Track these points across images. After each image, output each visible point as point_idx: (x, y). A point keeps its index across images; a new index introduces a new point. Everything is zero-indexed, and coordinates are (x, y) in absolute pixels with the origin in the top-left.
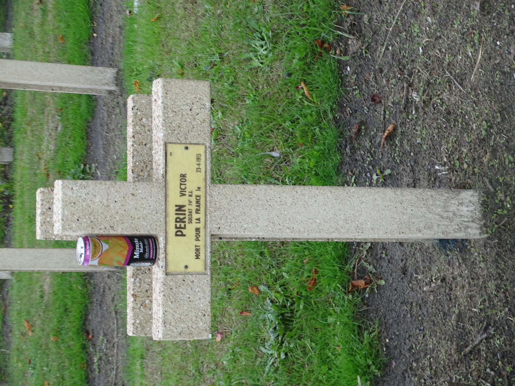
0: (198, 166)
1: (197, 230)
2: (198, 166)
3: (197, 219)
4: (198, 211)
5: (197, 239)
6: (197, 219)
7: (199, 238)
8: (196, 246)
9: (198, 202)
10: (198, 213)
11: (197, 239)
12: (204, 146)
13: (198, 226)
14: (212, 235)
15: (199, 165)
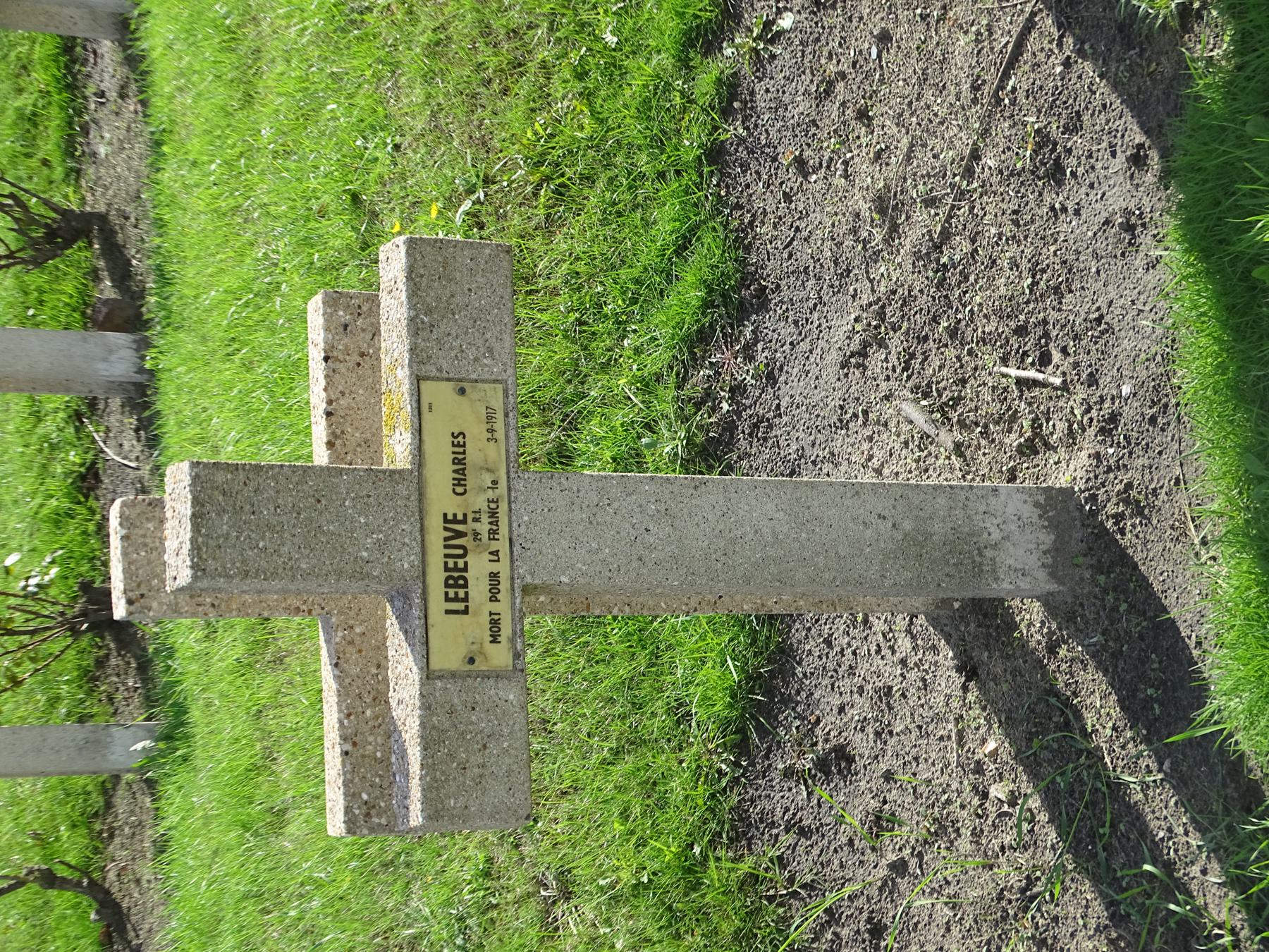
0: (490, 435)
1: (494, 576)
2: (490, 435)
3: (491, 553)
4: (493, 534)
5: (494, 599)
6: (491, 553)
7: (499, 596)
8: (491, 614)
9: (493, 514)
10: (494, 539)
11: (494, 599)
12: (500, 387)
13: (494, 567)
14: (526, 590)
15: (491, 431)
